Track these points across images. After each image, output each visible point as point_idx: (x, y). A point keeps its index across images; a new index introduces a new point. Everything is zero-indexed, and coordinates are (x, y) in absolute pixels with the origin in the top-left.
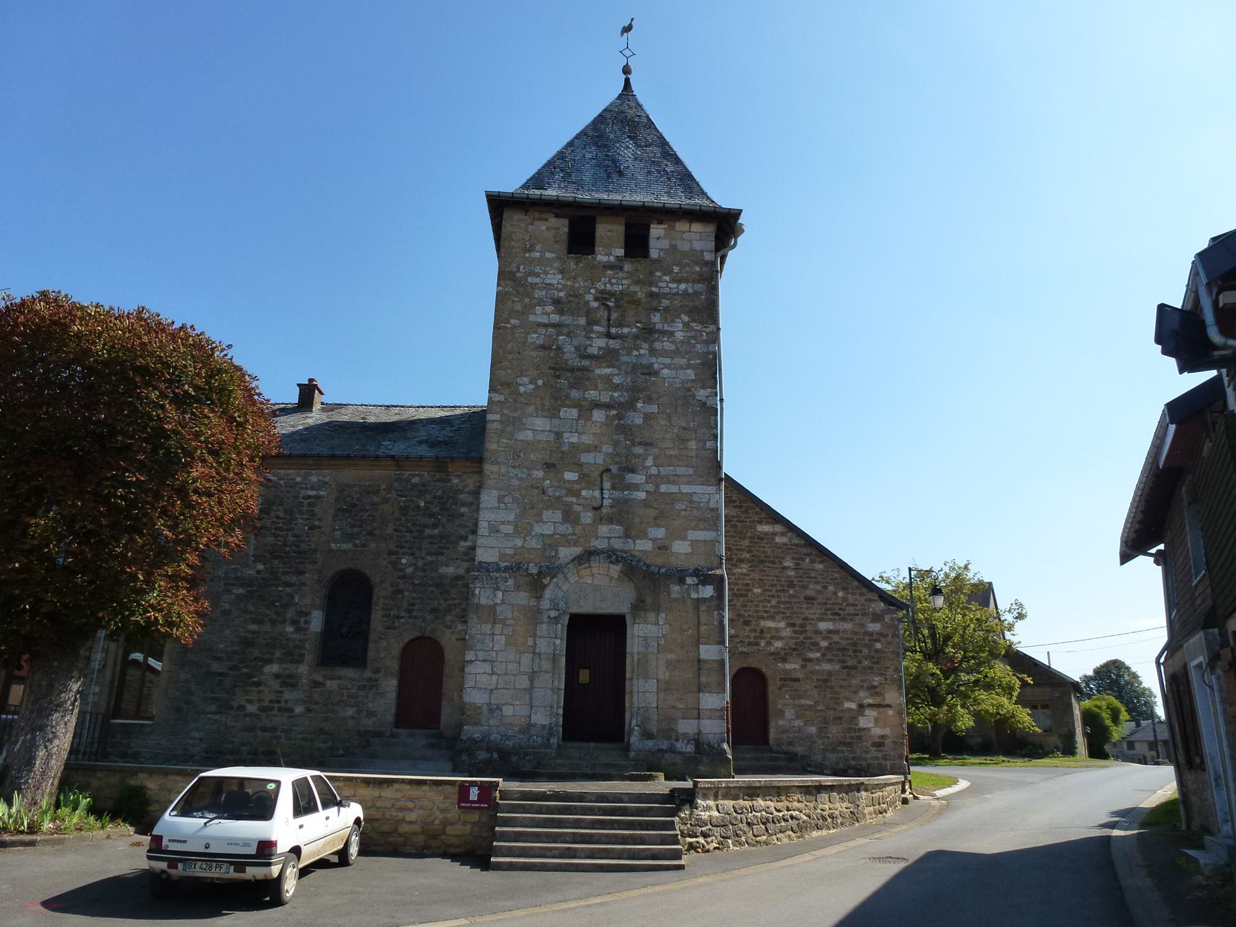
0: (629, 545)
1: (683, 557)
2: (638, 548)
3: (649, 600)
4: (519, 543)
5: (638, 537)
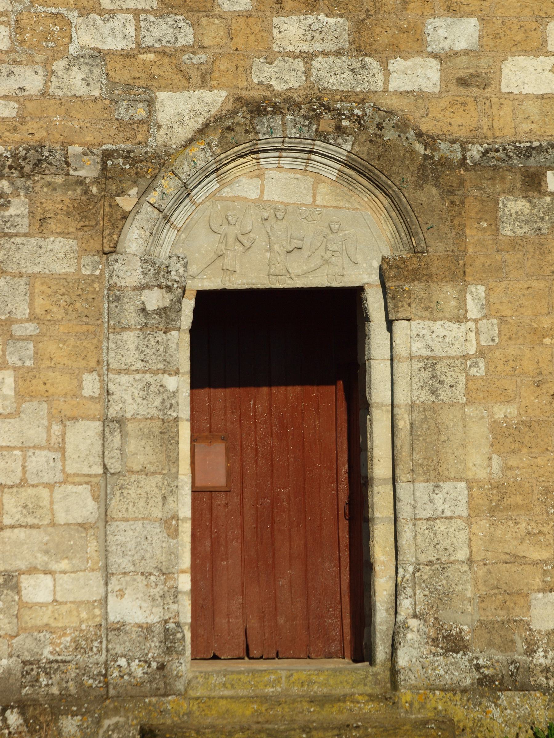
0: (373, 78)
1: (532, 108)
2: (397, 83)
3: (438, 248)
4: (32, 81)
5: (398, 51)
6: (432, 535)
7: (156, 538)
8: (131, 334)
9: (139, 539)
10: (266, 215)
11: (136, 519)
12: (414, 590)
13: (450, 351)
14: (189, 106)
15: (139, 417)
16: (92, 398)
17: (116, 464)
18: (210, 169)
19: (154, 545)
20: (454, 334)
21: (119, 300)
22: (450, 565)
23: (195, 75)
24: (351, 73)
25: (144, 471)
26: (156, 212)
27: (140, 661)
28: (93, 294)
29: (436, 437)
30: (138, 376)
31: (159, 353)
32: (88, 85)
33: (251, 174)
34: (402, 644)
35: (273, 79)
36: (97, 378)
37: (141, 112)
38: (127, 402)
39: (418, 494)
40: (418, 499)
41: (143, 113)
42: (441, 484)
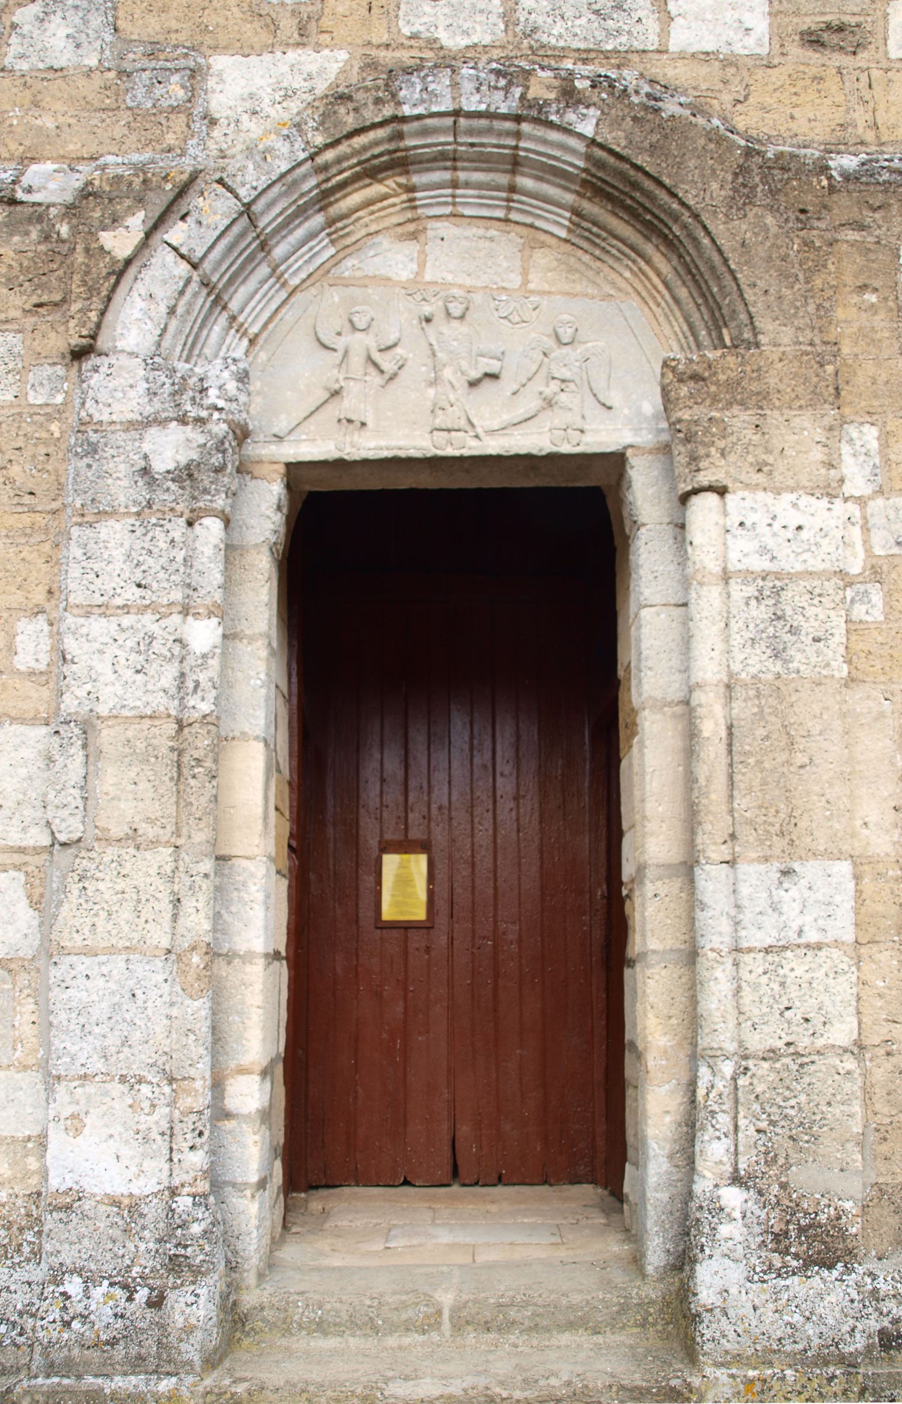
6: (776, 986)
7: (153, 994)
8: (118, 526)
9: (116, 999)
10: (427, 310)
11: (112, 950)
12: (735, 1118)
13: (811, 561)
14: (274, 80)
15: (126, 713)
16: (32, 673)
17: (71, 821)
18: (306, 186)
19: (149, 1012)
20: (818, 522)
21: (95, 451)
22: (815, 1058)
23: (288, 25)
24: (593, 17)
25: (133, 837)
26: (184, 267)
27: (111, 1285)
28: (46, 444)
29: (784, 757)
30: (127, 621)
31: (175, 566)
32: (78, 46)
33: (399, 230)
34: (707, 1251)
35: (441, 29)
36: (46, 628)
37: (175, 89)
38: (102, 679)
39: (744, 890)
40: (745, 903)
41: (181, 94)
42: (796, 866)
